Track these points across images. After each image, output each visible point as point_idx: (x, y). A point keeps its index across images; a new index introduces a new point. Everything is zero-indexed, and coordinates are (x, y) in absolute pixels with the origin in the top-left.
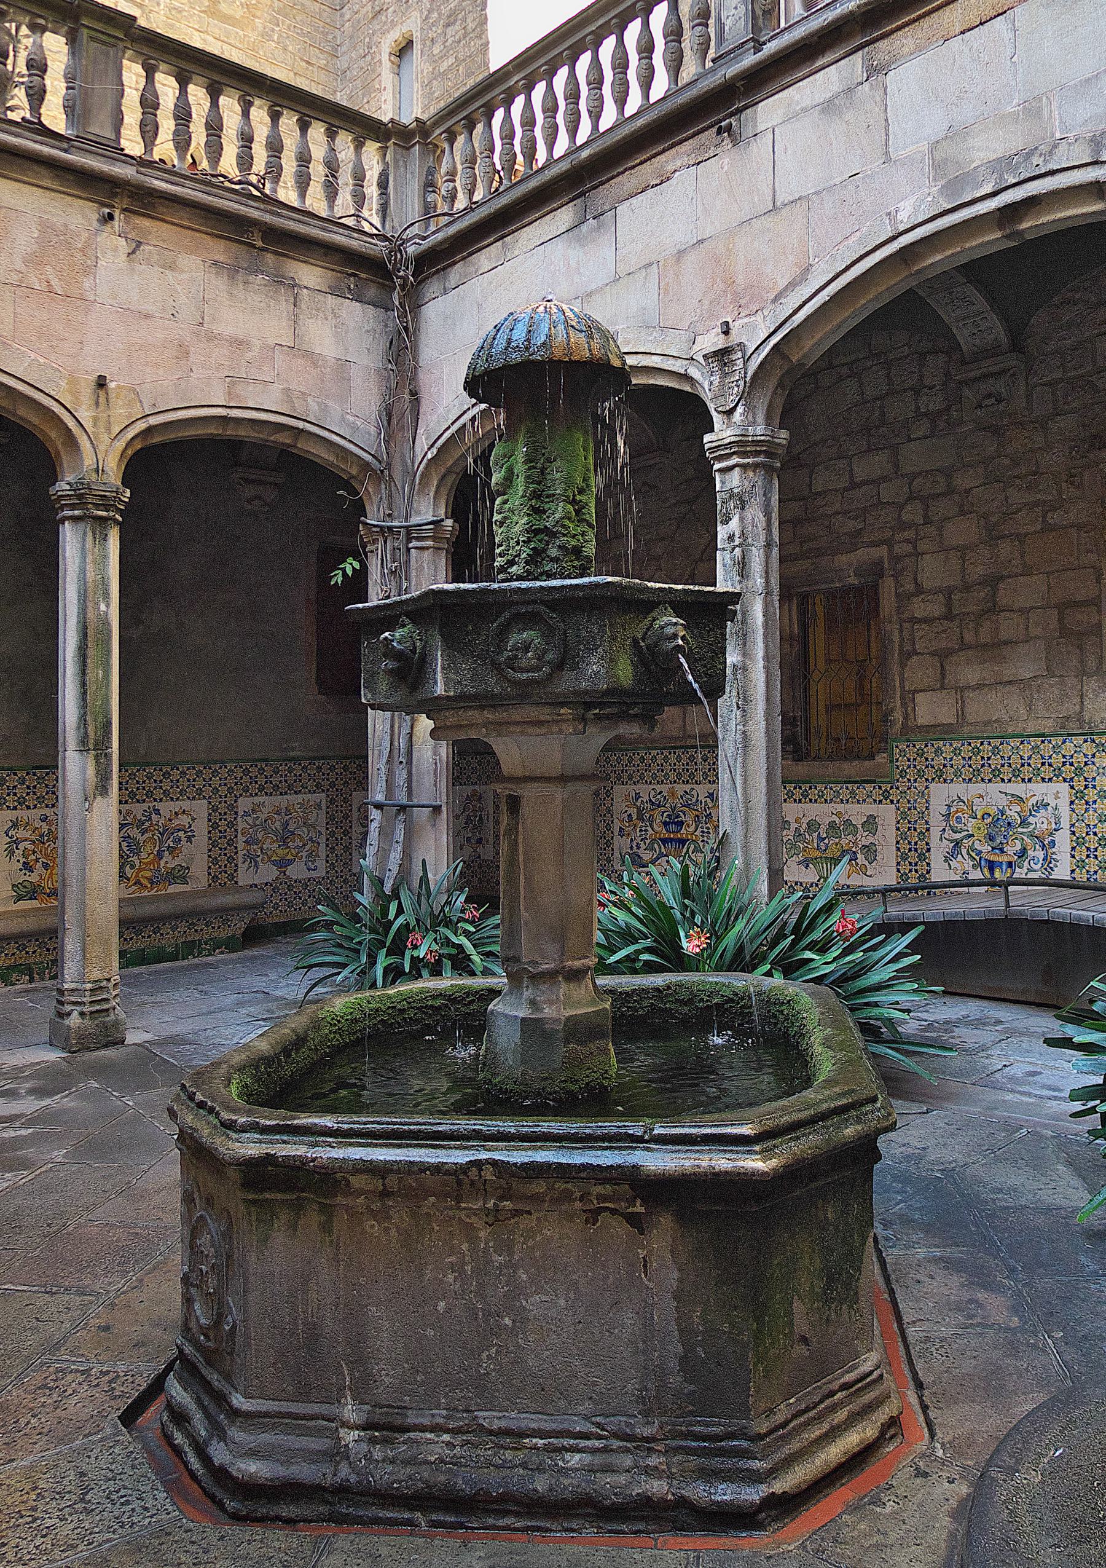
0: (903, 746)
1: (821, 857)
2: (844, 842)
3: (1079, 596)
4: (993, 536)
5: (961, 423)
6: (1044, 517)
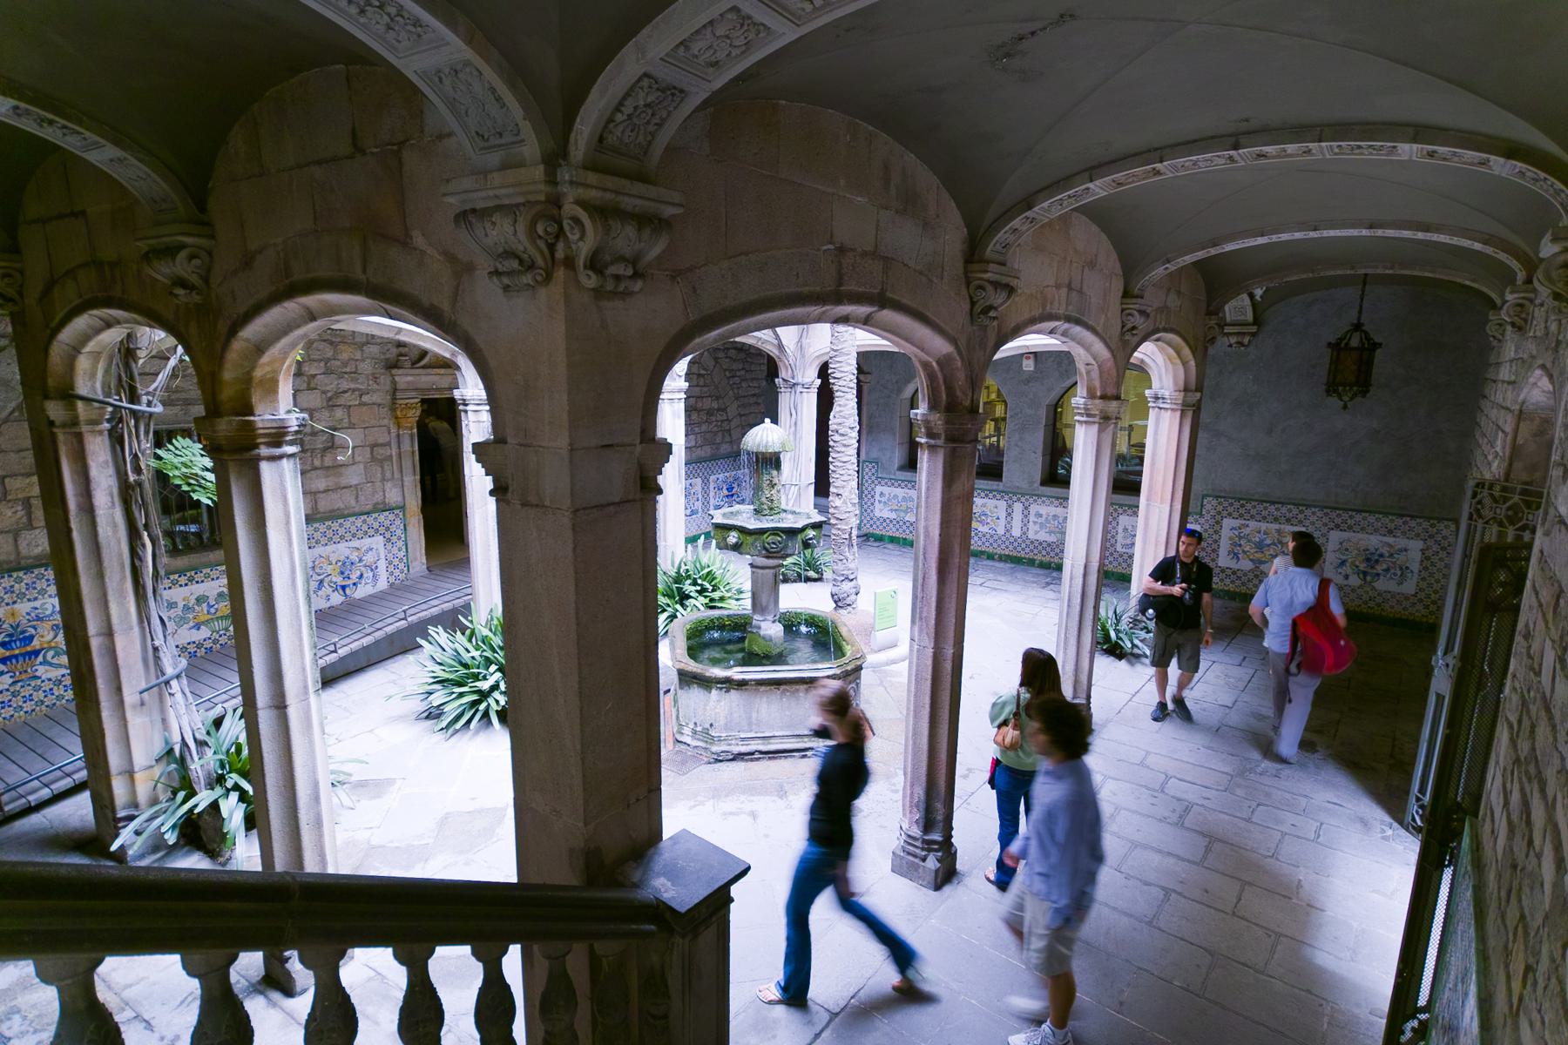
3: (381, 441)
4: (331, 404)
6: (361, 396)
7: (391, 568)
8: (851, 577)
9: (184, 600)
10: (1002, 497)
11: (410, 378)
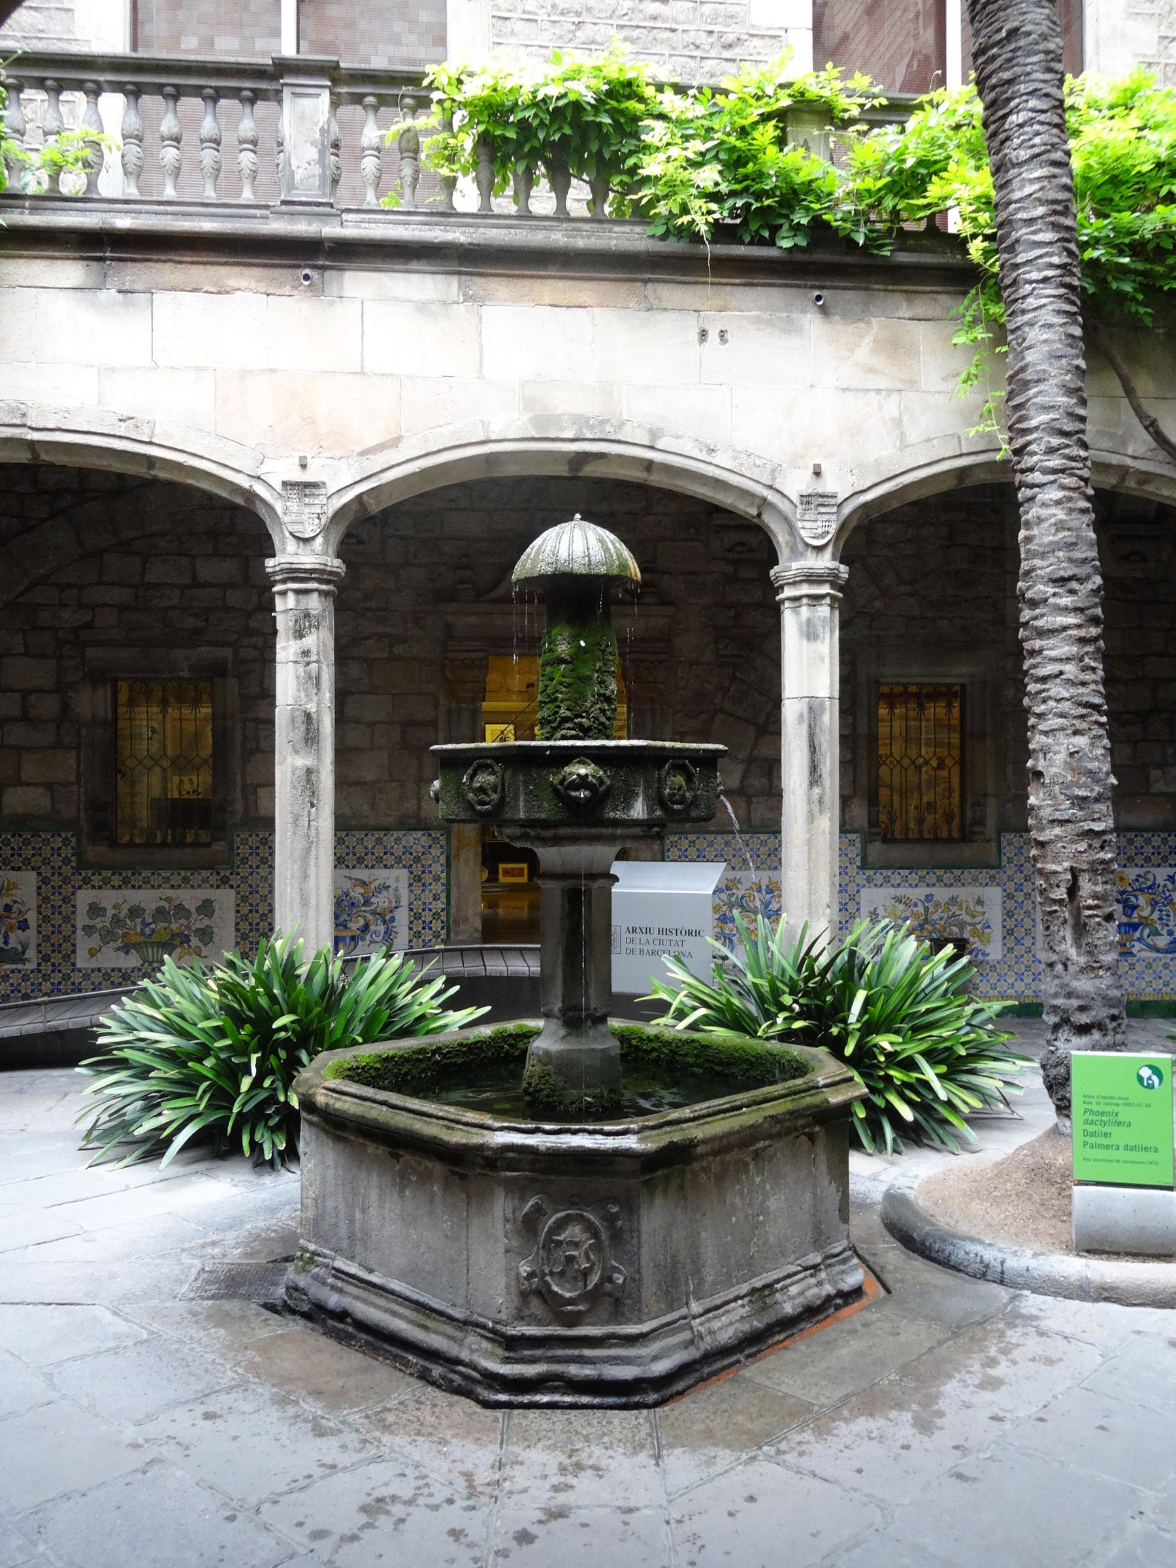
0: (245, 835)
1: (145, 943)
2: (174, 926)
6: (391, 646)
7: (418, 926)
9: (115, 907)
11: (473, 620)
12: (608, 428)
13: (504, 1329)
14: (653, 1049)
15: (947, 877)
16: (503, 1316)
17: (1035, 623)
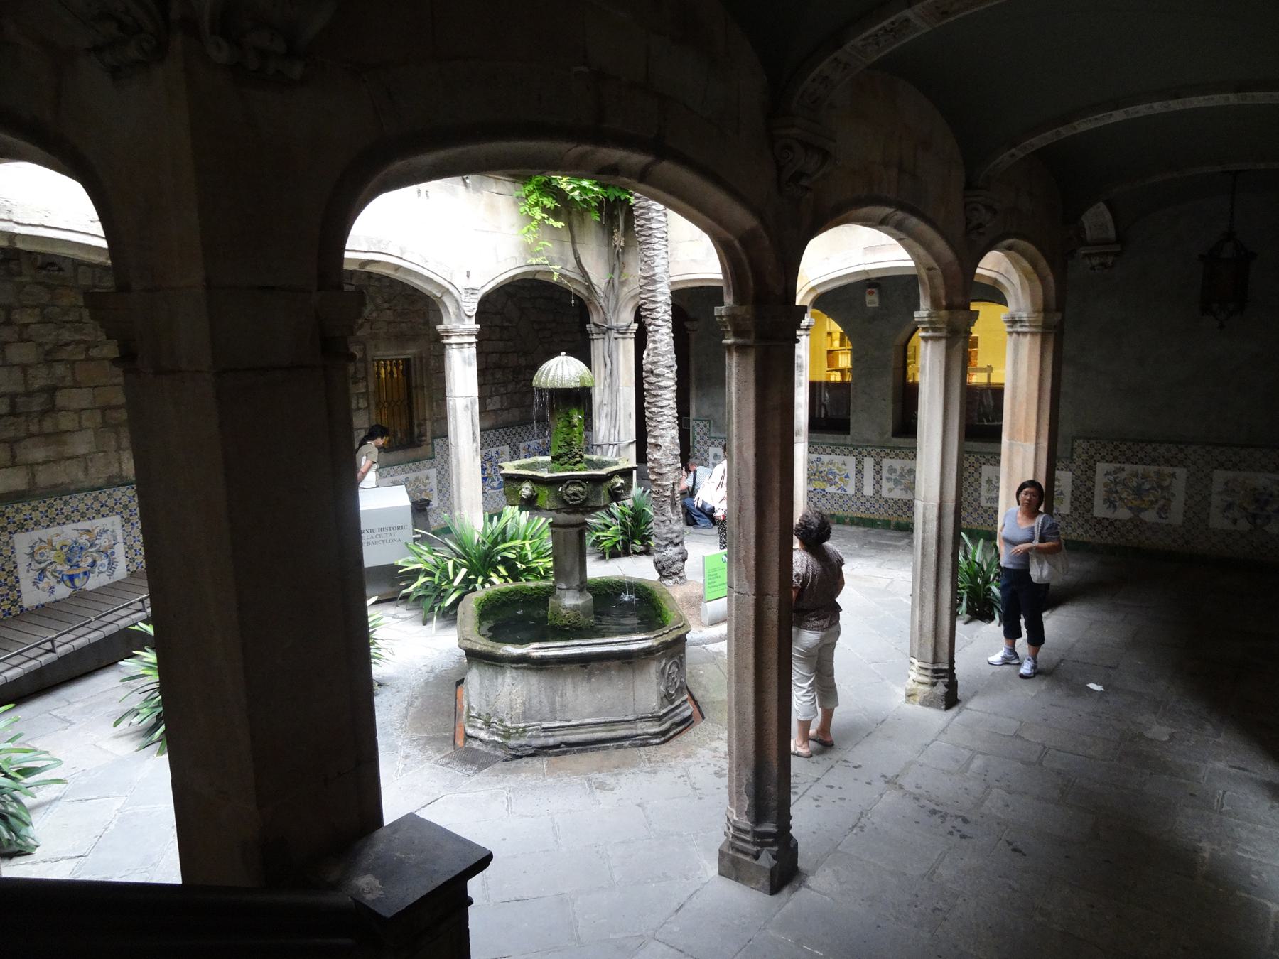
3: (114, 402)
4: (49, 358)
5: (20, 274)
6: (87, 349)
8: (677, 541)
10: (851, 452)
12: (382, 246)
13: (657, 714)
14: (536, 593)
15: (414, 467)
16: (656, 710)
17: (659, 384)
